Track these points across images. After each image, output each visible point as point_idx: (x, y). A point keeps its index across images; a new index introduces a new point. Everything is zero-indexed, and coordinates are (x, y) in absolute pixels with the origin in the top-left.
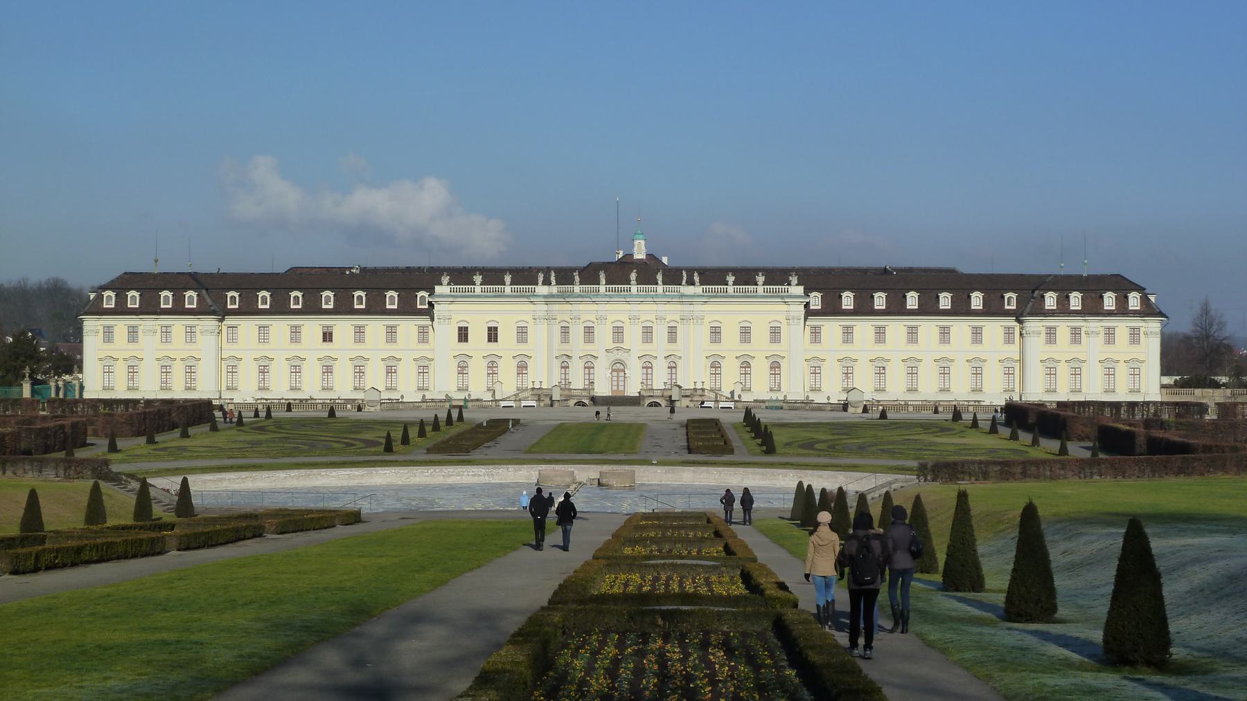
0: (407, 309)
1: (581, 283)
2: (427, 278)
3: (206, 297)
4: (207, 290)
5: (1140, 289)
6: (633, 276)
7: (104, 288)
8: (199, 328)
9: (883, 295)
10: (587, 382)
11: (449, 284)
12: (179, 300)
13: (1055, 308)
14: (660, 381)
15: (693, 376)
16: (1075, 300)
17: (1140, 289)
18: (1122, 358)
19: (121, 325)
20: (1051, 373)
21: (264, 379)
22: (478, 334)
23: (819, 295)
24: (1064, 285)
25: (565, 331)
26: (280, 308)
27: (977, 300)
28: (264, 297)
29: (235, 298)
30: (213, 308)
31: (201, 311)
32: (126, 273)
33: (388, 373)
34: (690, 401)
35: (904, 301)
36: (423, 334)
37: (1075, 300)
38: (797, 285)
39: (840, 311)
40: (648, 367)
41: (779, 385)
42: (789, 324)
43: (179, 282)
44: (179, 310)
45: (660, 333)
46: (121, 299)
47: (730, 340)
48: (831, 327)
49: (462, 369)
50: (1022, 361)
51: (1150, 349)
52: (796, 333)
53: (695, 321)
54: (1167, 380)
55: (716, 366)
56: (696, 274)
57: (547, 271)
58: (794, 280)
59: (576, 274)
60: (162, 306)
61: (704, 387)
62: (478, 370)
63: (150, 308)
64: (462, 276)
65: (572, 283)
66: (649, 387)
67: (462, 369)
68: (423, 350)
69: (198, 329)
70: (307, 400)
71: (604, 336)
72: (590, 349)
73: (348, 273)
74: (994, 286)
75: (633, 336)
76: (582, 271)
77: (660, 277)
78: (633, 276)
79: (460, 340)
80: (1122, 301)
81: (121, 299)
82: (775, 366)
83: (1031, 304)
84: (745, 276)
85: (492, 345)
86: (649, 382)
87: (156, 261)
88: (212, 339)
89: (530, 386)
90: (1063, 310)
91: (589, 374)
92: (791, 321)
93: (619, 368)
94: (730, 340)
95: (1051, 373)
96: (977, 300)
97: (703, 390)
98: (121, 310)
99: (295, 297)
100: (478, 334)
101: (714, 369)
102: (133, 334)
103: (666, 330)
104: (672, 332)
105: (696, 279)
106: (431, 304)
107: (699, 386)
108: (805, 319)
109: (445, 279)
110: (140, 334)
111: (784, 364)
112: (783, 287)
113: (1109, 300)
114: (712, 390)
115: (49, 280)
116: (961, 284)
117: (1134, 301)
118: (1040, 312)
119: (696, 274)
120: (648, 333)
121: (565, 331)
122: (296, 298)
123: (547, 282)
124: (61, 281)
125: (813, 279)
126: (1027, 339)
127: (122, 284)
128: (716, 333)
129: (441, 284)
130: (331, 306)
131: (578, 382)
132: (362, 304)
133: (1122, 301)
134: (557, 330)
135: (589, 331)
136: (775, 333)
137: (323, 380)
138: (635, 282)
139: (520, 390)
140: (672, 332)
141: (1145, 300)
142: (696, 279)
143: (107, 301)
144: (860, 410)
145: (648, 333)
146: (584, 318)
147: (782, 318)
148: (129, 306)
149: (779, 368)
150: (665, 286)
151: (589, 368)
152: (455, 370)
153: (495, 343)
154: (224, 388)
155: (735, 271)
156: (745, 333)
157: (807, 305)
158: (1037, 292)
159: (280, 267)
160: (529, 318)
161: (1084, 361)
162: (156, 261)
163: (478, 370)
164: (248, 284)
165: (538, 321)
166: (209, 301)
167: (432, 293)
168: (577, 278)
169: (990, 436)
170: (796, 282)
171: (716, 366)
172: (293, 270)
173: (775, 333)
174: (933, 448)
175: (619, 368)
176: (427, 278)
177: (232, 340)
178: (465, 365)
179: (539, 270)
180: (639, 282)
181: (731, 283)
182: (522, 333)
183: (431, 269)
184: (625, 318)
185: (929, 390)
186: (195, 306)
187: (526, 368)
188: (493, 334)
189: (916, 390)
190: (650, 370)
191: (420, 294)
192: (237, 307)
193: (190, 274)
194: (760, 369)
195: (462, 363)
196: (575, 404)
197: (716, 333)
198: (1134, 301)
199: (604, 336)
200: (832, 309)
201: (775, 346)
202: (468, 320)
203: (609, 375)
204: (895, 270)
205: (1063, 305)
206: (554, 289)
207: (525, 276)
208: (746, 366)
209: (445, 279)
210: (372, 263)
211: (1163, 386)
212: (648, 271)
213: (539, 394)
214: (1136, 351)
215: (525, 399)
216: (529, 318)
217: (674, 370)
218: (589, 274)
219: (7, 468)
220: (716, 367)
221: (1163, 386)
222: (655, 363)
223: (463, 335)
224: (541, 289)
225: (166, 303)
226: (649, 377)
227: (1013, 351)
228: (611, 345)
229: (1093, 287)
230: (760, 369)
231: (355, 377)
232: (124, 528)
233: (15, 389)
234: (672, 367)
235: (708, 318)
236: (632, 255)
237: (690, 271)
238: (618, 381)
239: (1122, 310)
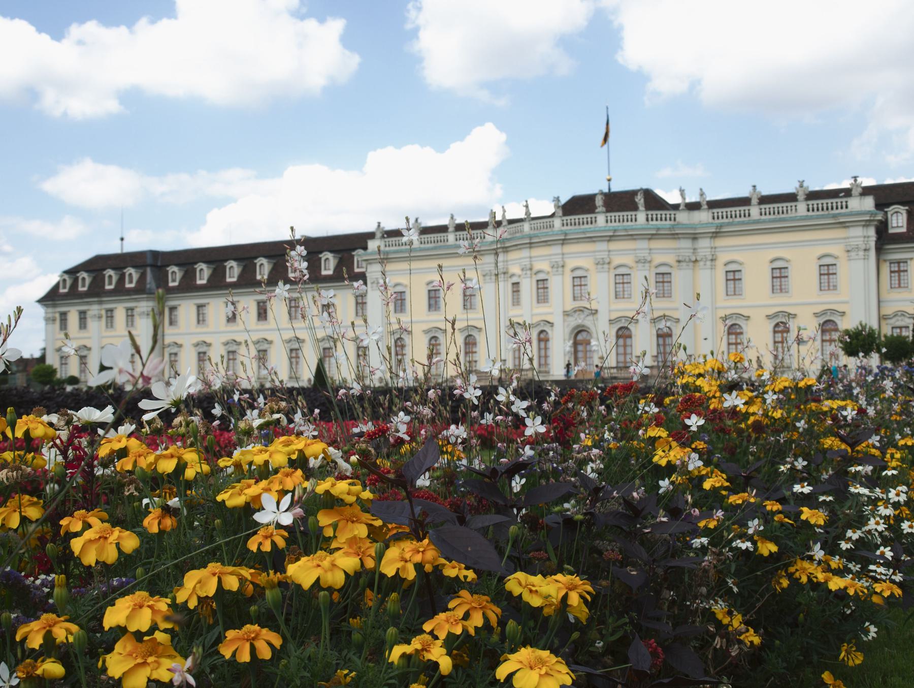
22: (418, 300)
29: (175, 273)
44: (120, 291)
55: (734, 330)
63: (97, 291)
69: (89, 314)
100: (418, 300)
101: (734, 337)
102: (83, 317)
112: (839, 200)
120: (622, 280)
128: (733, 277)
135: (542, 285)
140: (663, 278)
150: (650, 213)
180: (608, 211)
187: (475, 344)
203: (568, 349)
228: (570, 305)
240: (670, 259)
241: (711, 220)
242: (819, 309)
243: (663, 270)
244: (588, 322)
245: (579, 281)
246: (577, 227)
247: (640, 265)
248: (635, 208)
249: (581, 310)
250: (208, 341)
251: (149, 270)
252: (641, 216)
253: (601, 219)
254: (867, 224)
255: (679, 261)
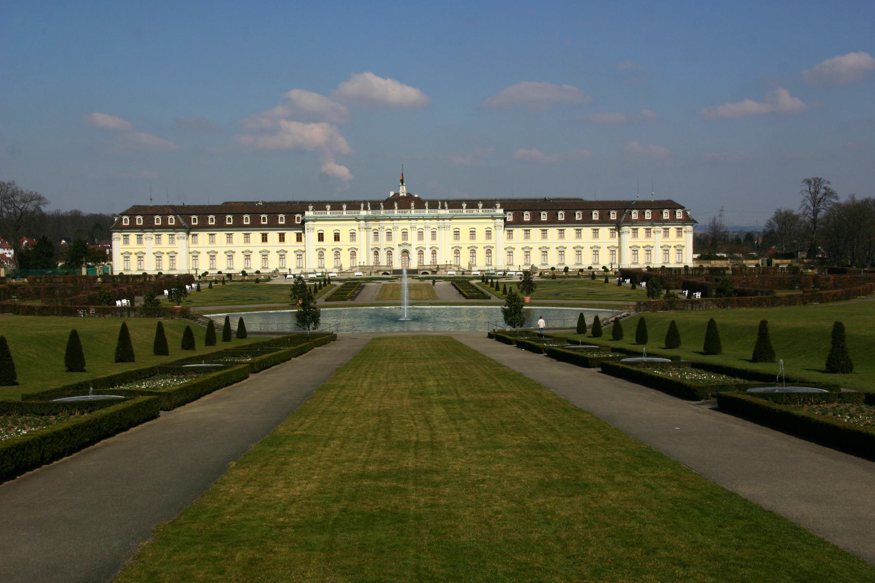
0: (290, 225)
1: (385, 209)
2: (302, 207)
3: (180, 218)
4: (180, 215)
5: (682, 208)
6: (413, 204)
7: (123, 214)
8: (176, 236)
9: (546, 213)
10: (388, 262)
11: (313, 210)
12: (165, 220)
13: (637, 218)
14: (427, 260)
15: (445, 257)
16: (648, 215)
17: (682, 208)
18: (673, 245)
19: (133, 236)
20: (635, 252)
21: (213, 263)
23: (511, 213)
24: (642, 206)
25: (376, 234)
26: (221, 226)
27: (595, 216)
28: (195, 220)
30: (183, 225)
31: (177, 228)
32: (134, 206)
33: (280, 258)
34: (445, 271)
35: (608, 216)
36: (299, 238)
37: (648, 215)
38: (500, 208)
39: (609, 220)
40: (421, 253)
41: (491, 262)
42: (496, 229)
43: (164, 211)
44: (165, 227)
45: (427, 234)
46: (133, 220)
47: (465, 240)
48: (518, 232)
49: (321, 255)
50: (619, 247)
51: (687, 239)
52: (500, 234)
53: (446, 228)
54: (696, 256)
55: (457, 252)
56: (446, 203)
57: (365, 202)
58: (498, 205)
59: (381, 204)
60: (156, 224)
61: (452, 264)
62: (329, 256)
63: (149, 226)
64: (319, 206)
65: (379, 208)
66: (422, 264)
67: (321, 255)
68: (300, 246)
70: (238, 274)
71: (397, 237)
72: (390, 244)
73: (257, 205)
74: (605, 207)
75: (413, 237)
76: (384, 202)
77: (426, 205)
78: (413, 204)
79: (335, 240)
80: (673, 214)
81: (133, 220)
82: (489, 252)
83: (624, 216)
84: (472, 204)
85: (337, 243)
86: (422, 262)
87: (151, 199)
88: (184, 241)
89: (359, 265)
90: (642, 221)
91: (390, 258)
92: (497, 228)
93: (406, 252)
94: (465, 240)
95: (635, 252)
96: (595, 216)
97: (451, 265)
98: (132, 227)
99: (194, 219)
103: (430, 233)
104: (434, 234)
105: (446, 205)
106: (303, 222)
107: (449, 263)
108: (505, 227)
109: (311, 207)
110: (144, 239)
111: (493, 251)
113: (666, 215)
114: (455, 266)
115: (72, 211)
116: (587, 207)
117: (679, 215)
118: (629, 222)
119: (446, 203)
120: (421, 235)
121: (376, 234)
122: (264, 219)
123: (366, 208)
124: (78, 211)
125: (508, 205)
126: (623, 236)
127: (133, 212)
128: (457, 233)
129: (308, 210)
130: (249, 223)
131: (383, 261)
132: (248, 222)
133: (673, 214)
134: (371, 234)
135: (389, 234)
136: (488, 233)
137: (233, 264)
138: (413, 208)
139: (352, 268)
140: (434, 234)
141: (685, 213)
142: (446, 205)
143: (138, 221)
144: (537, 274)
145: (421, 235)
146: (386, 227)
147: (492, 226)
148: (137, 224)
149: (491, 253)
151: (390, 254)
152: (317, 257)
153: (338, 242)
154: (191, 268)
155: (466, 201)
156: (473, 233)
157: (505, 219)
158: (627, 210)
159: (218, 201)
160: (356, 228)
161: (652, 247)
162: (151, 199)
163: (329, 256)
164: (203, 212)
165: (361, 230)
166: (181, 221)
167: (303, 214)
168: (382, 206)
169: (619, 287)
170: (499, 206)
171: (457, 252)
172: (226, 203)
173: (488, 233)
174: (594, 294)
175: (406, 252)
176: (302, 207)
177: (195, 242)
178: (322, 254)
179: (360, 202)
180: (415, 209)
181: (464, 207)
182: (353, 235)
183: (301, 202)
184: (408, 227)
185: (587, 262)
186: (174, 224)
187: (355, 255)
188: (337, 238)
189: (581, 263)
190: (422, 256)
191: (297, 216)
192: (197, 224)
193: (170, 206)
194: (481, 254)
195: (321, 253)
196: (382, 274)
197: (457, 233)
198: (679, 215)
199: (397, 237)
200: (518, 222)
201: (489, 241)
202: (475, 227)
203: (400, 258)
204: (551, 200)
205: (641, 217)
206: (370, 213)
207: (354, 206)
208: (473, 251)
209: (311, 207)
210: (268, 199)
211: (694, 259)
212: (405, 202)
213: (362, 268)
214: (680, 241)
215: (356, 271)
216: (356, 228)
217: (435, 255)
218: (389, 204)
219: (131, 312)
220: (456, 253)
221: (694, 259)
222: (424, 251)
223: (321, 237)
224: (363, 213)
225: (158, 222)
226: (422, 259)
227: (615, 242)
228: (401, 242)
229: (657, 207)
230: (481, 254)
231: (263, 261)
232: (373, 333)
233: (78, 270)
234: (434, 253)
235: (453, 227)
236: (399, 194)
237: (443, 202)
238: (405, 261)
239: (673, 220)
240: (423, 227)
241: (449, 213)
242: (485, 245)
243: (420, 230)
244: (408, 248)
245: (405, 234)
246: (404, 214)
247: (426, 229)
248: (424, 208)
249: (405, 244)
250: (285, 250)
251: (178, 216)
252: (427, 211)
253: (413, 211)
254: (501, 218)
255: (439, 228)
